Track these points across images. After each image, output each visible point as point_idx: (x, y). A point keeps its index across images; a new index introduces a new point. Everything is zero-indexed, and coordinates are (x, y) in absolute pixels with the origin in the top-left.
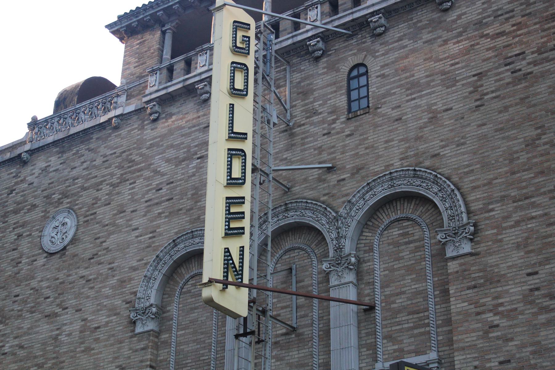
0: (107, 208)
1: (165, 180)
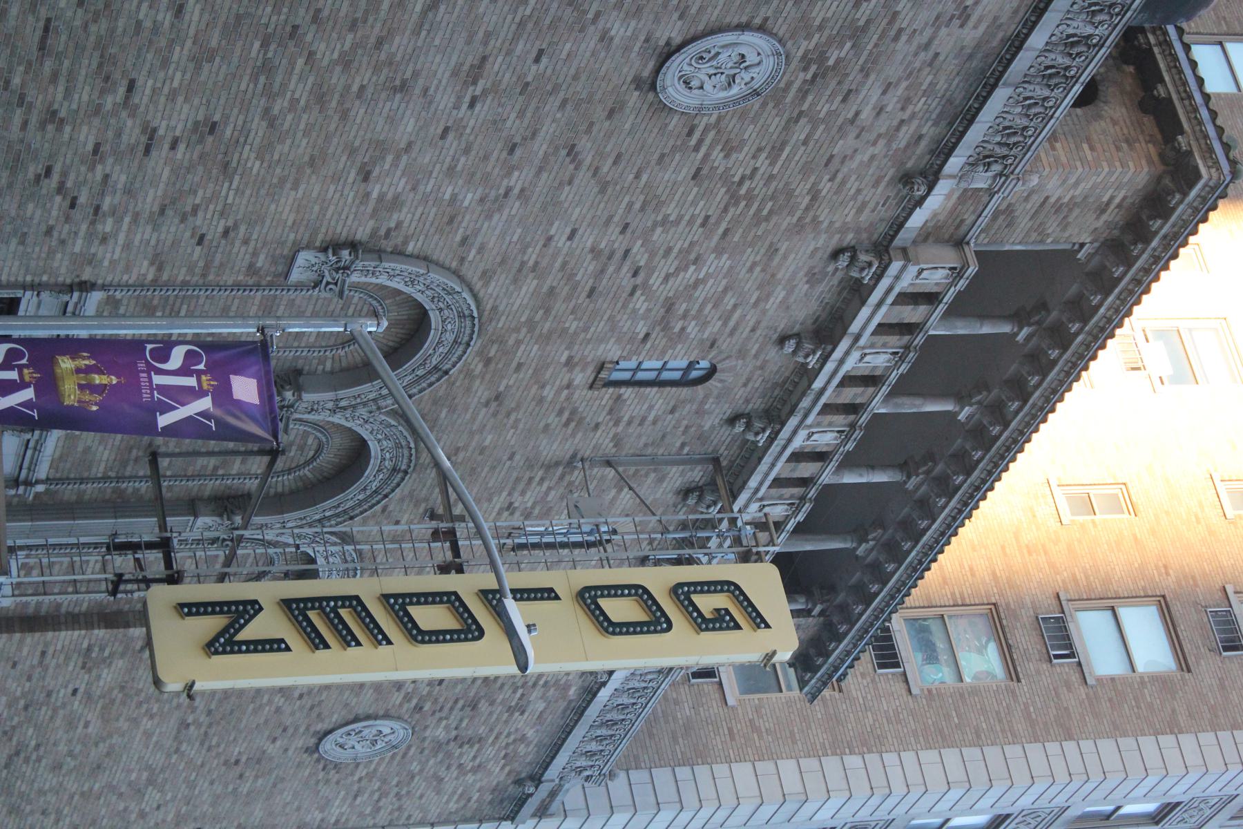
0: (686, 172)
1: (651, 282)
